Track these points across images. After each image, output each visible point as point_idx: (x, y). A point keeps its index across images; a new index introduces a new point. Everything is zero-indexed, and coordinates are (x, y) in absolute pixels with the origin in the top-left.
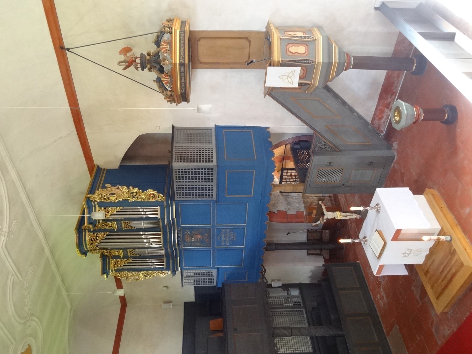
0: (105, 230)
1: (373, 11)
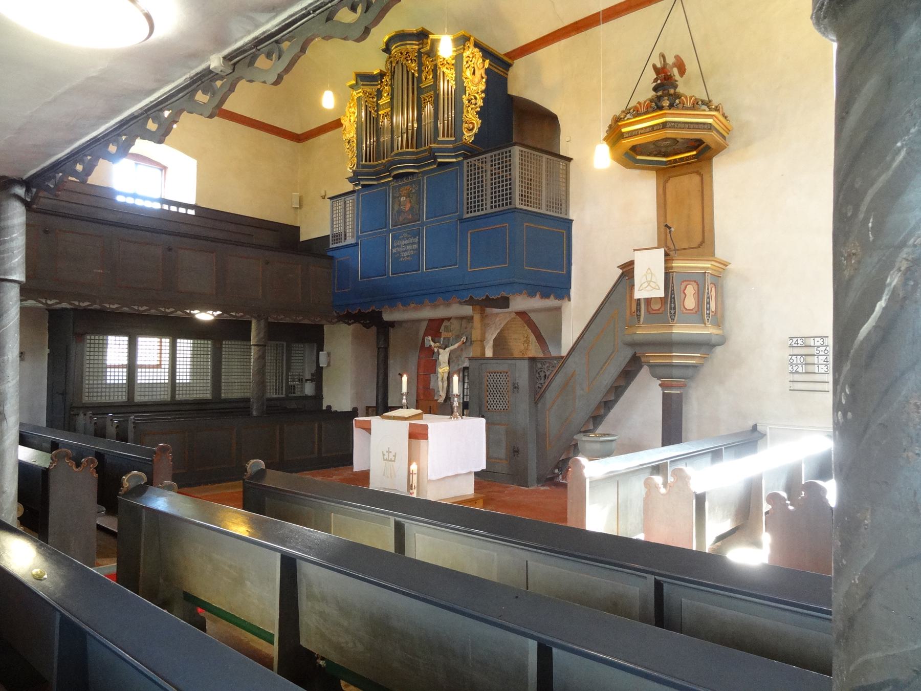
0: (420, 71)
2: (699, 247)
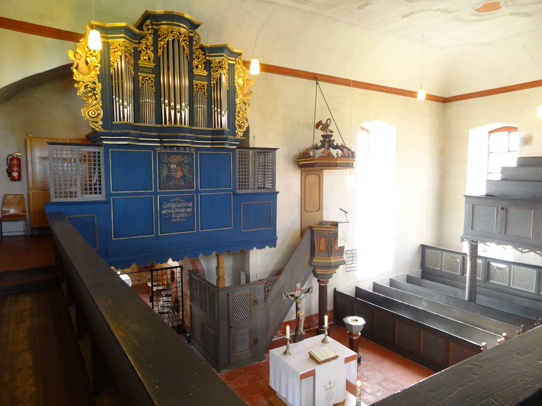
1: (333, 288)
2: (318, 211)
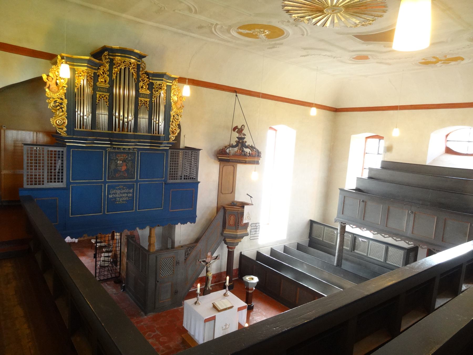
1: (239, 252)
